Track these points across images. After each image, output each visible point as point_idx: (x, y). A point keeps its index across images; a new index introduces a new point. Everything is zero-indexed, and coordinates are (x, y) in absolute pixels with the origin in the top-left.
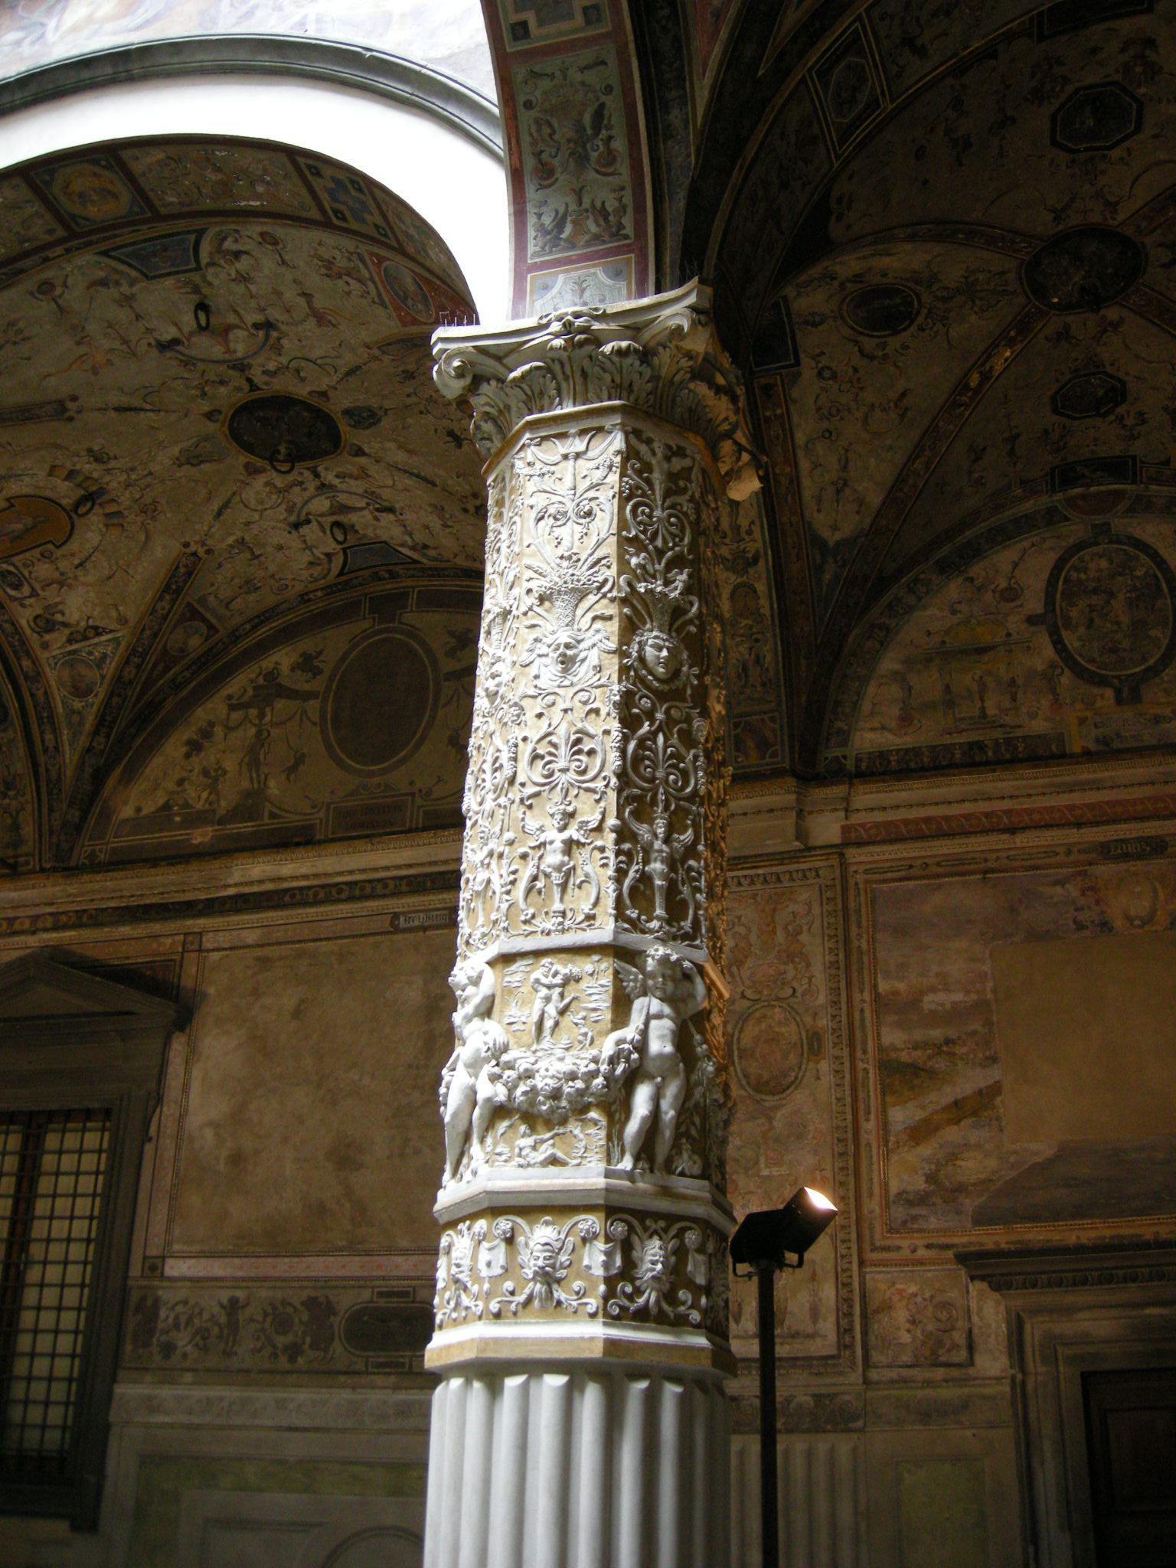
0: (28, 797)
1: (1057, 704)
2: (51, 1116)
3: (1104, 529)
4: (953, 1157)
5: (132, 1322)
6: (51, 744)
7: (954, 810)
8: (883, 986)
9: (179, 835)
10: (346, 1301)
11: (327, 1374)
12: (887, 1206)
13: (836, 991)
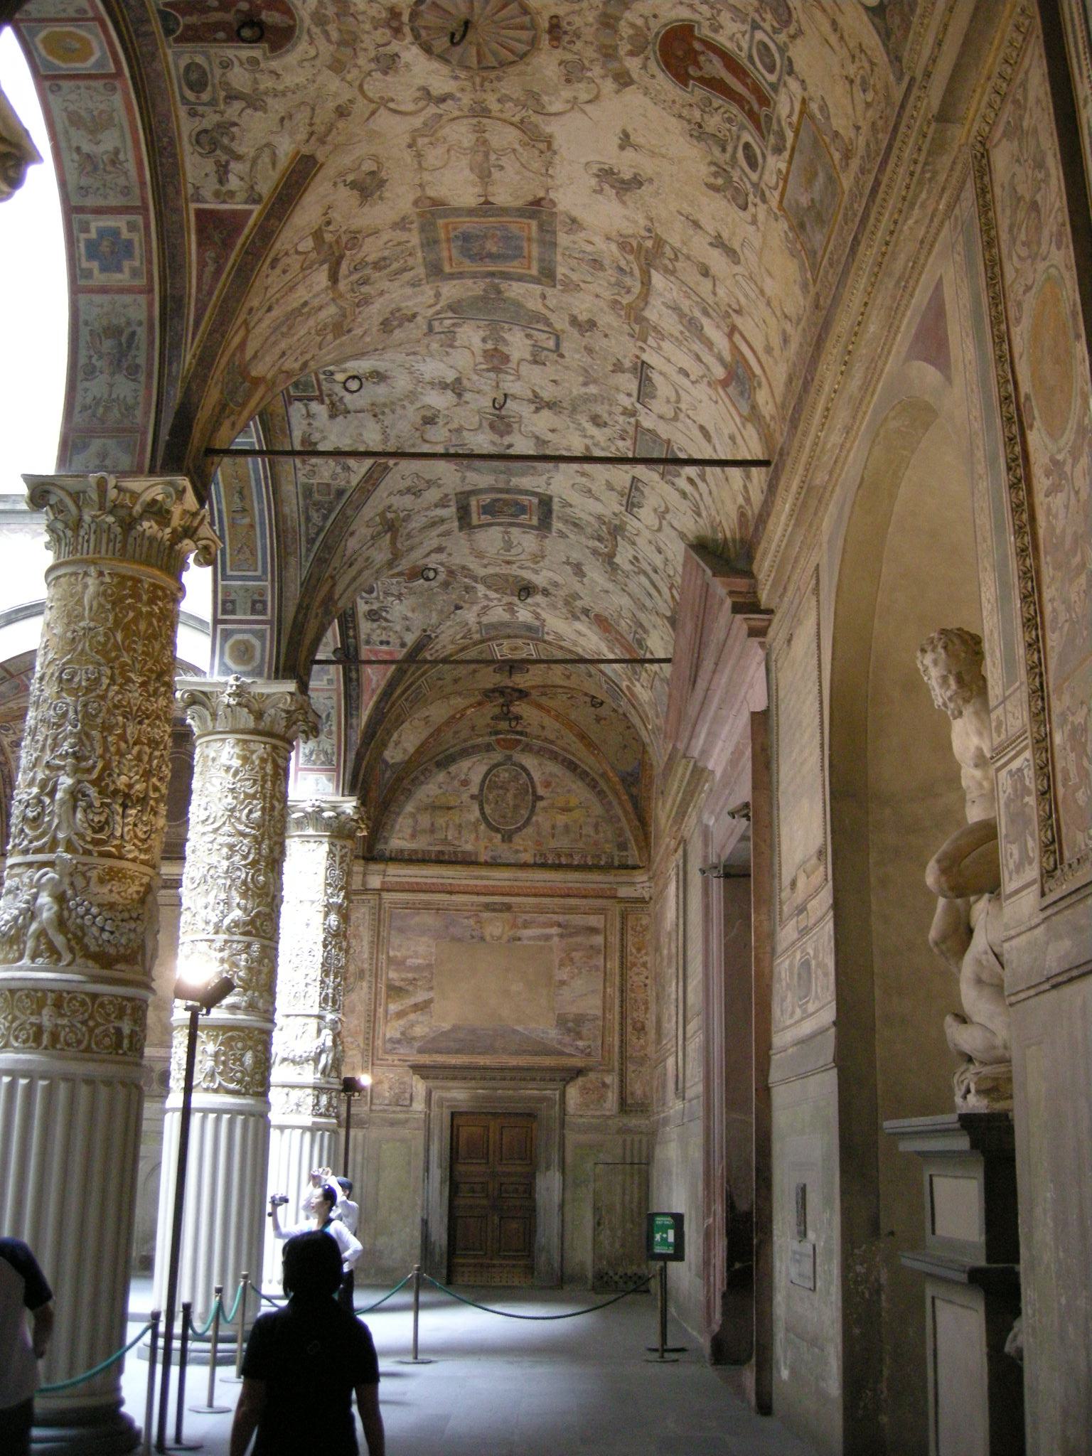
1: (477, 838)
3: (509, 758)
4: (412, 1026)
7: (429, 881)
8: (391, 954)
12: (384, 1043)
13: (371, 953)
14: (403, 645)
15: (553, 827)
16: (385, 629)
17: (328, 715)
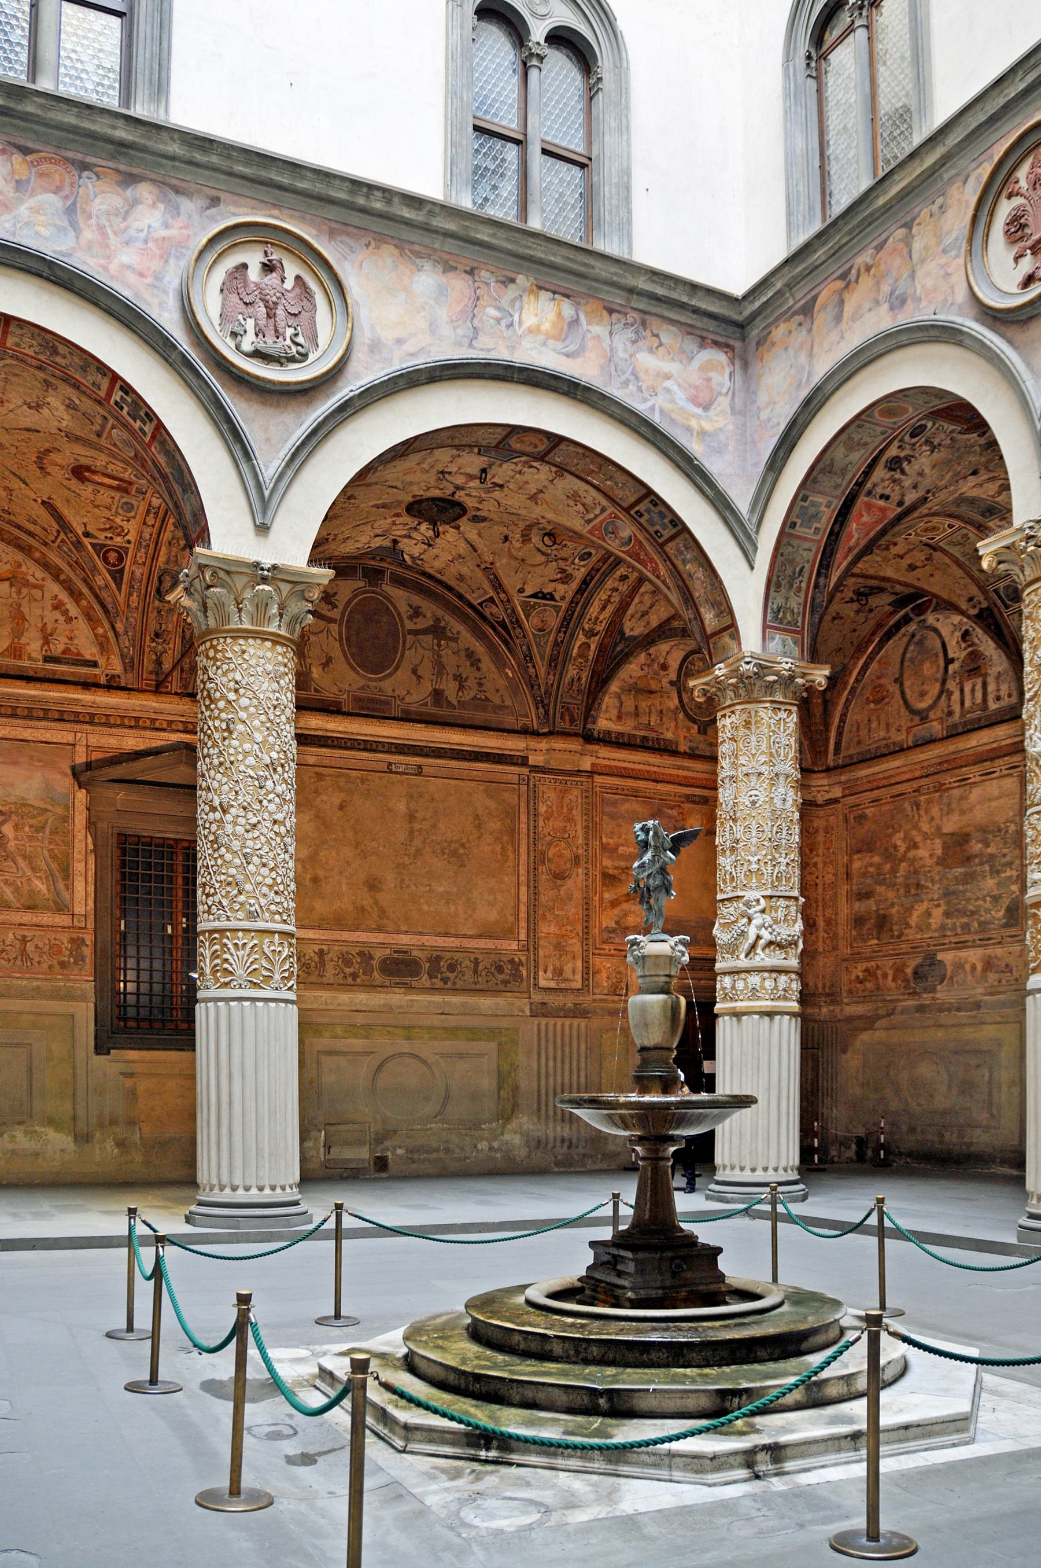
0: (171, 646)
4: (625, 915)
16: (894, 481)
17: (801, 570)
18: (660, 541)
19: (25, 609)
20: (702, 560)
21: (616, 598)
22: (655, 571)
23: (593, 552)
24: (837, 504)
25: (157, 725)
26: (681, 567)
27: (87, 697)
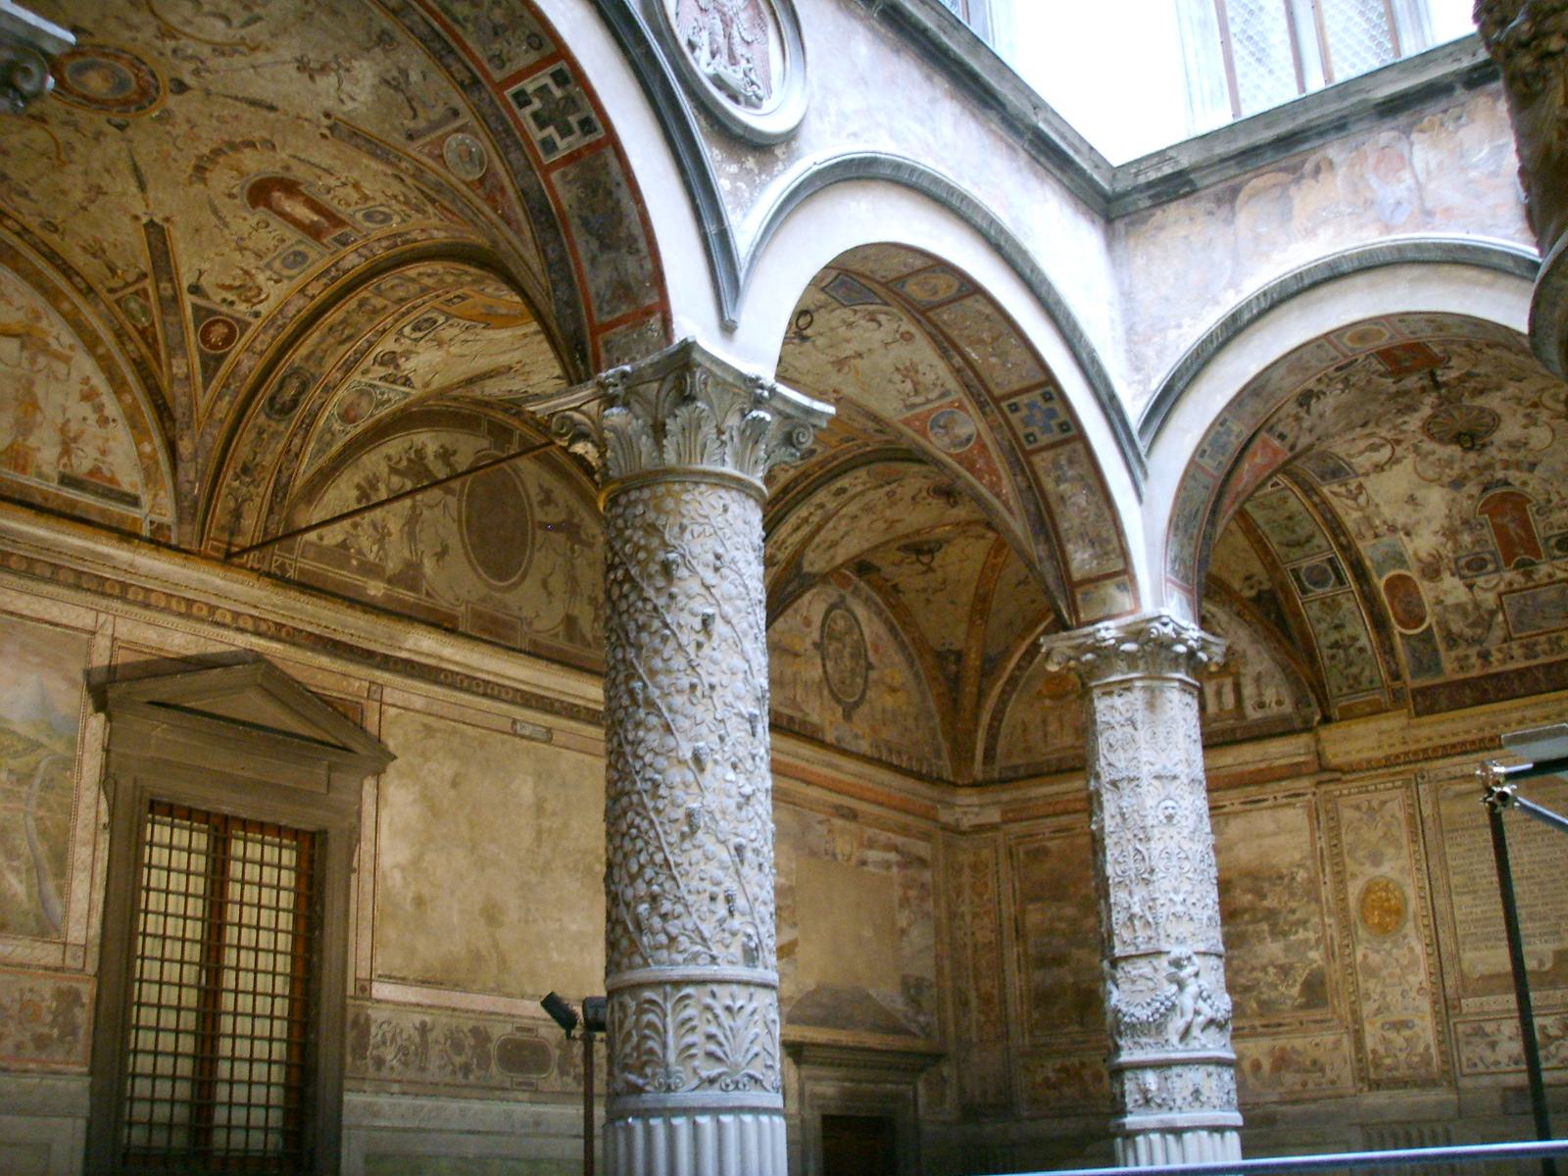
0: (261, 490)
2: (245, 825)
5: (351, 1036)
6: (294, 449)
9: (358, 580)
10: (499, 1031)
11: (488, 1090)
14: (1292, 448)
15: (884, 711)
18: (1028, 447)
19: (39, 392)
20: (1092, 481)
21: (815, 519)
22: (995, 488)
23: (819, 450)
24: (1246, 434)
25: (218, 617)
26: (1049, 484)
27: (122, 554)
